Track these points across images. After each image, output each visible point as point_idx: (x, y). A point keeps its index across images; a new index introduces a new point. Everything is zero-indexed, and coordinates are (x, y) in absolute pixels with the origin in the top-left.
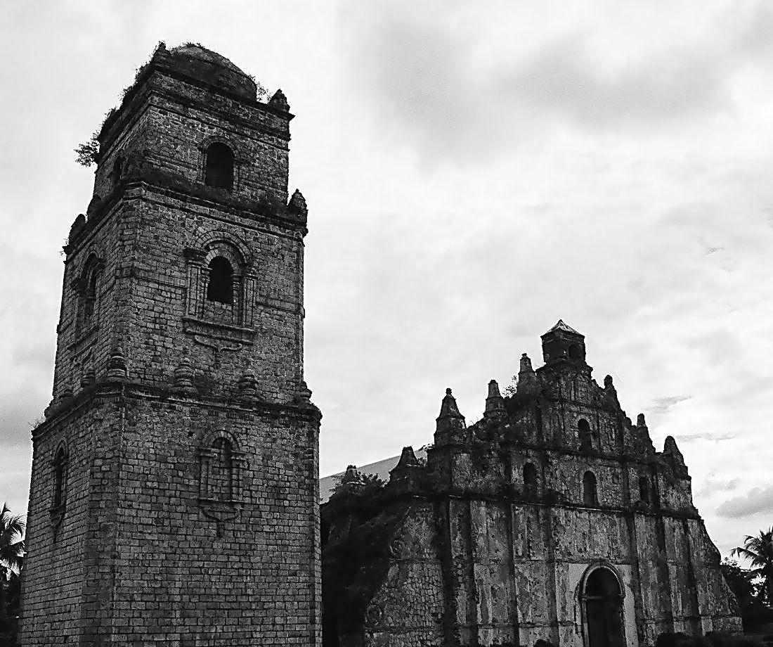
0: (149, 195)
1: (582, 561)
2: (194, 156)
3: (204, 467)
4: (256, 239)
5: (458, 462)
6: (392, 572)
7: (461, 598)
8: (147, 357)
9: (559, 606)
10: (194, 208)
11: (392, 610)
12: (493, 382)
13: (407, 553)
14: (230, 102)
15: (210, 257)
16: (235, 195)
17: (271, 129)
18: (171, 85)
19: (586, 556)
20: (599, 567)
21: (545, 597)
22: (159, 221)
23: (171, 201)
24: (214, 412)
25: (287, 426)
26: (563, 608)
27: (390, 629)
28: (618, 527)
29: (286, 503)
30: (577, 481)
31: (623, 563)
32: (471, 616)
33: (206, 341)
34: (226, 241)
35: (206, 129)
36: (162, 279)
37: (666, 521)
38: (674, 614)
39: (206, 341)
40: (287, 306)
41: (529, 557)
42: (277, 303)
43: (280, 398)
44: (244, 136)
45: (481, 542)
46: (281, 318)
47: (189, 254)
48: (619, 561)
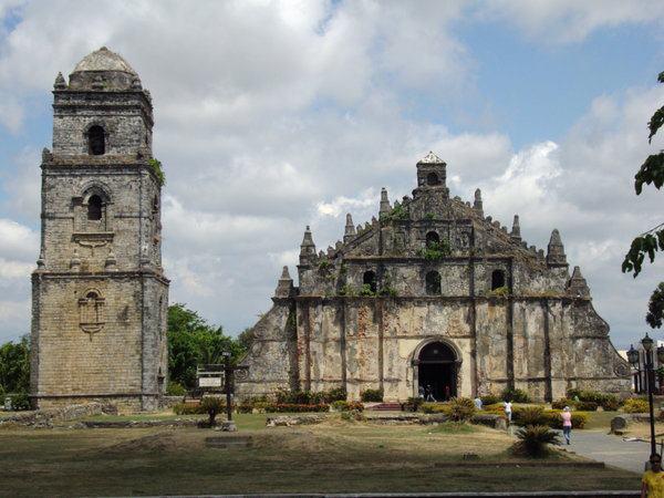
1: (418, 337)
2: (79, 139)
7: (302, 363)
8: (57, 256)
9: (386, 368)
15: (87, 198)
26: (390, 370)
31: (464, 337)
32: (308, 374)
33: (87, 243)
34: (94, 186)
35: (86, 120)
36: (62, 215)
37: (517, 306)
38: (517, 376)
39: (87, 243)
40: (134, 214)
42: (128, 215)
43: (130, 266)
45: (316, 328)
46: (130, 222)
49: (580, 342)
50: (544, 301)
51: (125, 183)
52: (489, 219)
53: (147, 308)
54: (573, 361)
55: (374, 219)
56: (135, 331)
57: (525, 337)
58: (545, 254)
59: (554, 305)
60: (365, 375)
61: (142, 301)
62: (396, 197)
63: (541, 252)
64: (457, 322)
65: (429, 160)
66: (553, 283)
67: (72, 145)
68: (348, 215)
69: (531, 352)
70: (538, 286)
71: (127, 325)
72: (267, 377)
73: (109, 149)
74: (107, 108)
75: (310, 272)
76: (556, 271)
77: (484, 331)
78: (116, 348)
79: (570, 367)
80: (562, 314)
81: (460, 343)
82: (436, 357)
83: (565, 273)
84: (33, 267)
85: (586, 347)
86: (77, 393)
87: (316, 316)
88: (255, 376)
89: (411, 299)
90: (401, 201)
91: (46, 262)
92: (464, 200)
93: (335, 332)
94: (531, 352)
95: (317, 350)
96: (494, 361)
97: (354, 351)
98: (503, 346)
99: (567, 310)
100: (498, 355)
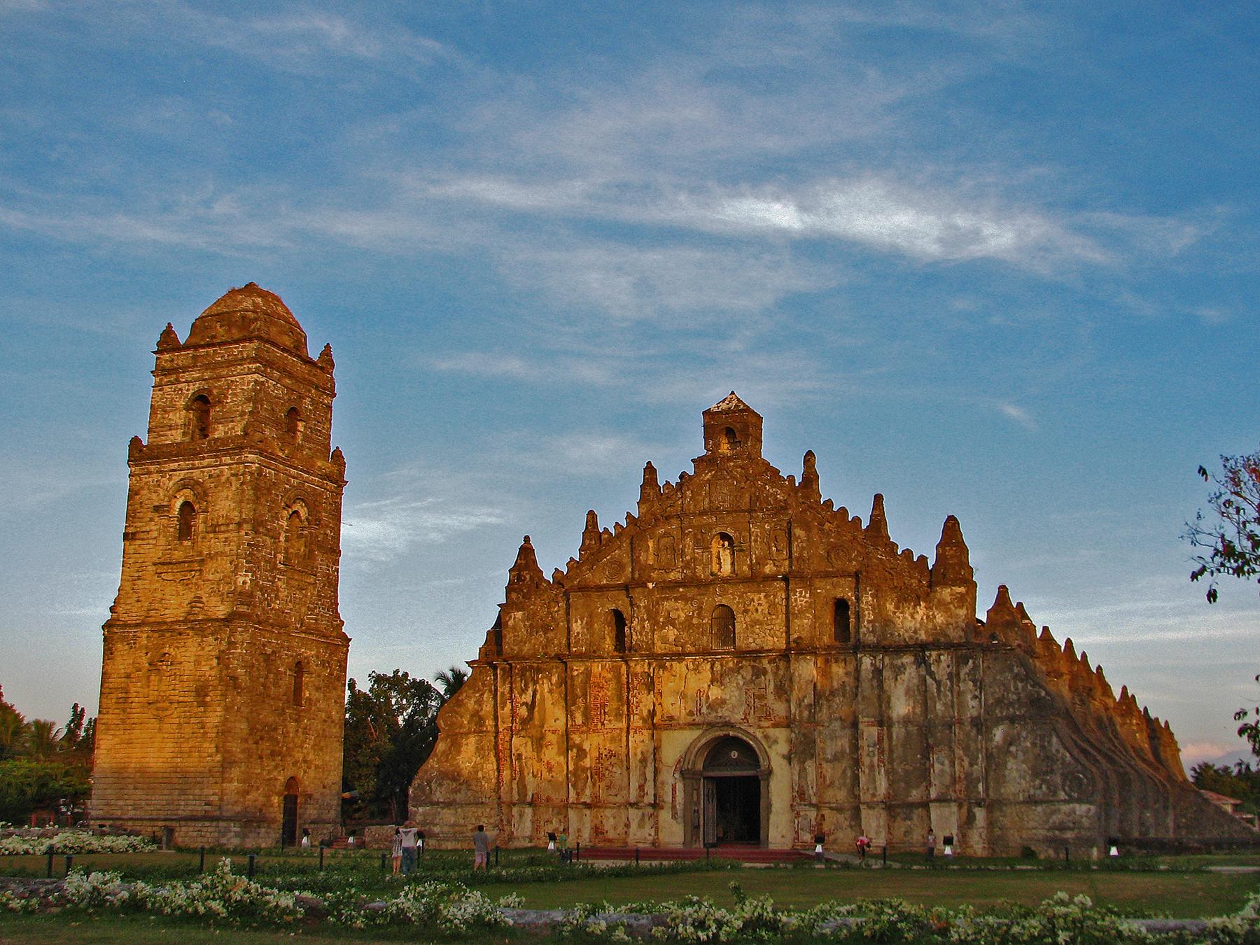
0: (137, 470)
1: (693, 725)
3: (153, 678)
4: (210, 476)
5: (511, 623)
6: (441, 746)
10: (167, 467)
11: (441, 785)
12: (591, 513)
13: (461, 726)
14: (211, 350)
15: (178, 504)
16: (211, 436)
17: (243, 359)
18: (166, 361)
19: (698, 719)
20: (721, 733)
21: (625, 773)
22: (142, 488)
23: (152, 468)
24: (162, 633)
25: (212, 634)
26: (641, 787)
27: (438, 803)
28: (770, 676)
29: (208, 699)
30: (695, 621)
31: (775, 726)
36: (142, 536)
37: (867, 661)
38: (865, 797)
41: (603, 724)
42: (223, 528)
44: (218, 378)
47: (157, 509)
48: (764, 724)
49: (998, 734)
50: (919, 650)
51: (223, 479)
52: (829, 503)
53: (234, 678)
54: (979, 769)
55: (629, 516)
56: (215, 717)
57: (883, 721)
58: (931, 563)
59: (938, 661)
60: (602, 794)
61: (227, 667)
62: (668, 475)
63: (923, 559)
64: (762, 697)
65: (724, 406)
66: (940, 619)
67: (171, 428)
68: (591, 513)
69: (899, 752)
70: (912, 621)
71: (203, 704)
72: (459, 797)
73: (216, 430)
74: (219, 365)
75: (519, 614)
76: (946, 593)
77: (806, 713)
78: (191, 744)
79: (971, 781)
80: (954, 677)
81: (766, 737)
82: (737, 763)
83: (969, 599)
84: (108, 615)
85: (1010, 741)
86: (139, 814)
87: (523, 691)
88: (439, 796)
89: (680, 656)
90: (674, 481)
91: (120, 609)
92: (784, 474)
93: (555, 717)
94: (899, 752)
95: (522, 750)
96: (828, 770)
97: (582, 753)
98: (844, 743)
99: (965, 670)
100: (836, 758)
